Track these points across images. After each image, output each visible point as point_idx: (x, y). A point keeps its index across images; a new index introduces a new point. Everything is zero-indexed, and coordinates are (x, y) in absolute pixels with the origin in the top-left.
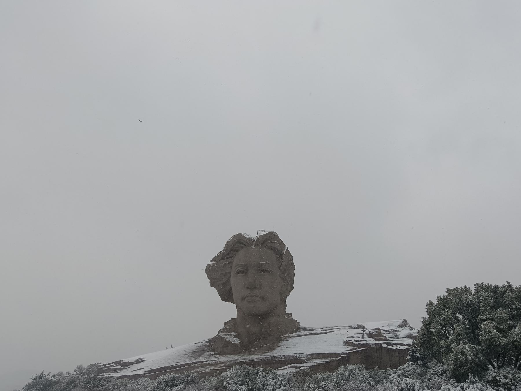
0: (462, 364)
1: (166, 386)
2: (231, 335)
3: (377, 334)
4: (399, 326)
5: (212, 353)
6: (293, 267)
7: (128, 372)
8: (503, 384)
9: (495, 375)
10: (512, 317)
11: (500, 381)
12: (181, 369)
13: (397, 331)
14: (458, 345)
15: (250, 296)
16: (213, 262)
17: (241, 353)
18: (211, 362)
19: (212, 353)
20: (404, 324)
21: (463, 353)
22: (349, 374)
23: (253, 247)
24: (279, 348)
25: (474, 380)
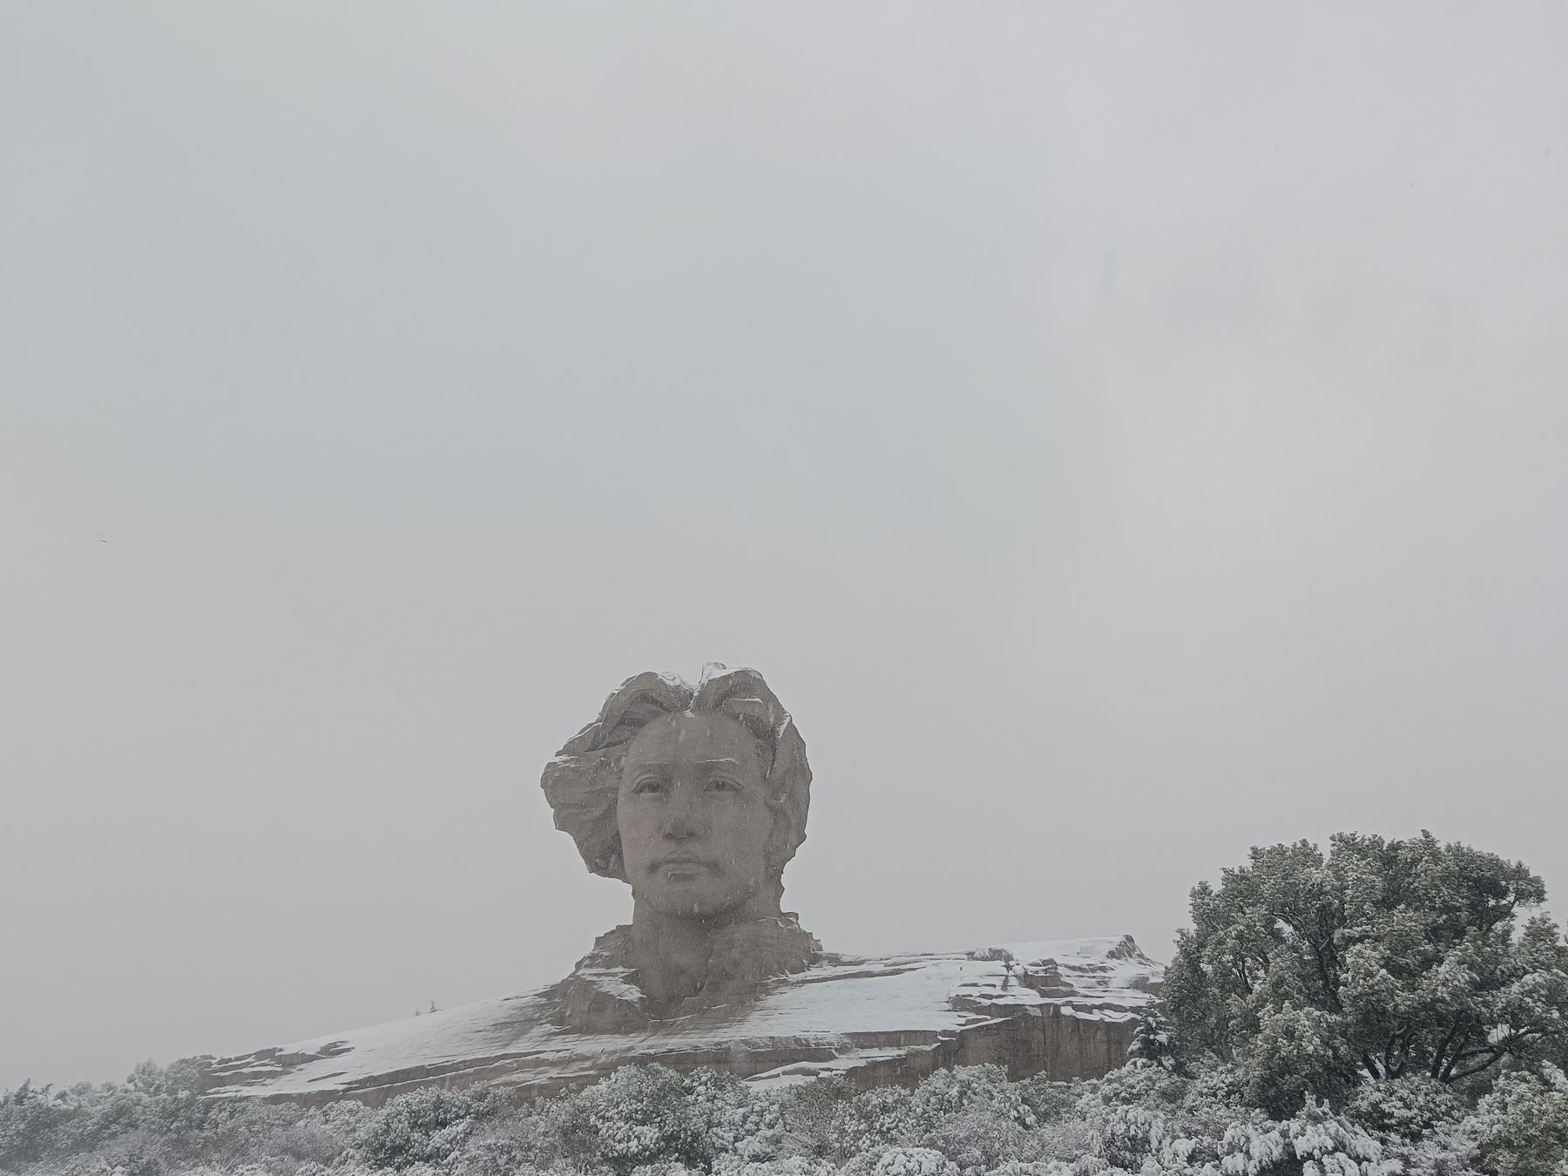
0: (1287, 1067)
1: (414, 1126)
2: (614, 975)
3: (1045, 979)
4: (1112, 955)
5: (554, 1029)
6: (806, 776)
7: (295, 1083)
8: (1399, 1124)
9: (1377, 1096)
10: (1434, 933)
11: (1391, 1115)
12: (460, 1076)
13: (1103, 969)
14: (1279, 1010)
15: (674, 861)
16: (564, 757)
17: (644, 1029)
18: (551, 1056)
19: (554, 1029)
20: (1126, 949)
21: (1290, 1034)
22: (962, 1094)
23: (688, 713)
24: (756, 1015)
25: (1318, 1110)
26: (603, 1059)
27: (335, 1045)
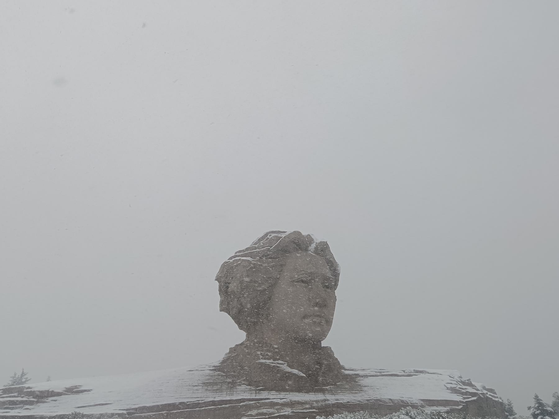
18: (279, 401)
26: (315, 404)
27: (76, 387)
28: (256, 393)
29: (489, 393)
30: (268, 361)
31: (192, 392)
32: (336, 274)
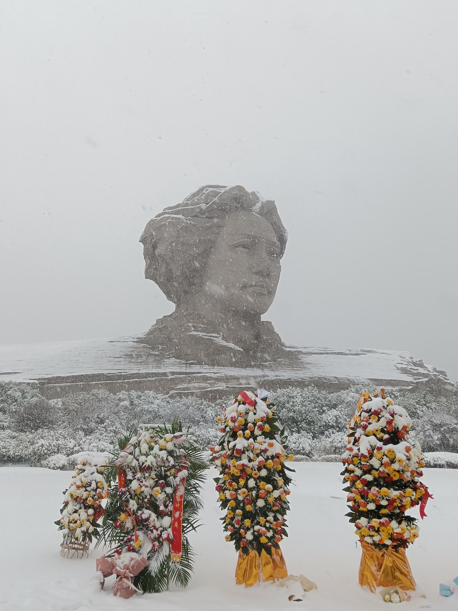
28: (186, 367)
29: (441, 375)
30: (201, 334)
31: (113, 363)
32: (282, 240)
